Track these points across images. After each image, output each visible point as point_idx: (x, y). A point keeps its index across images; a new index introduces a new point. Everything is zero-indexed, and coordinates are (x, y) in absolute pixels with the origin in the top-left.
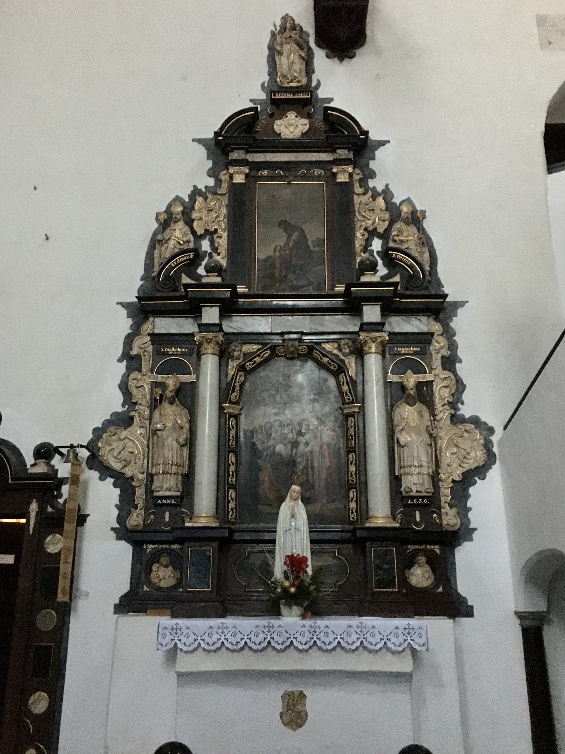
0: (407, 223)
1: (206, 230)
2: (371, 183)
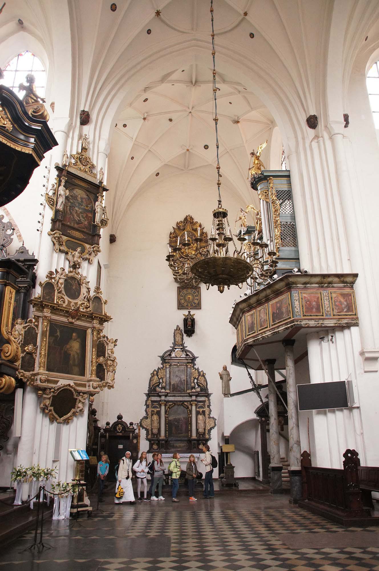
0: (202, 376)
1: (161, 377)
2: (195, 367)
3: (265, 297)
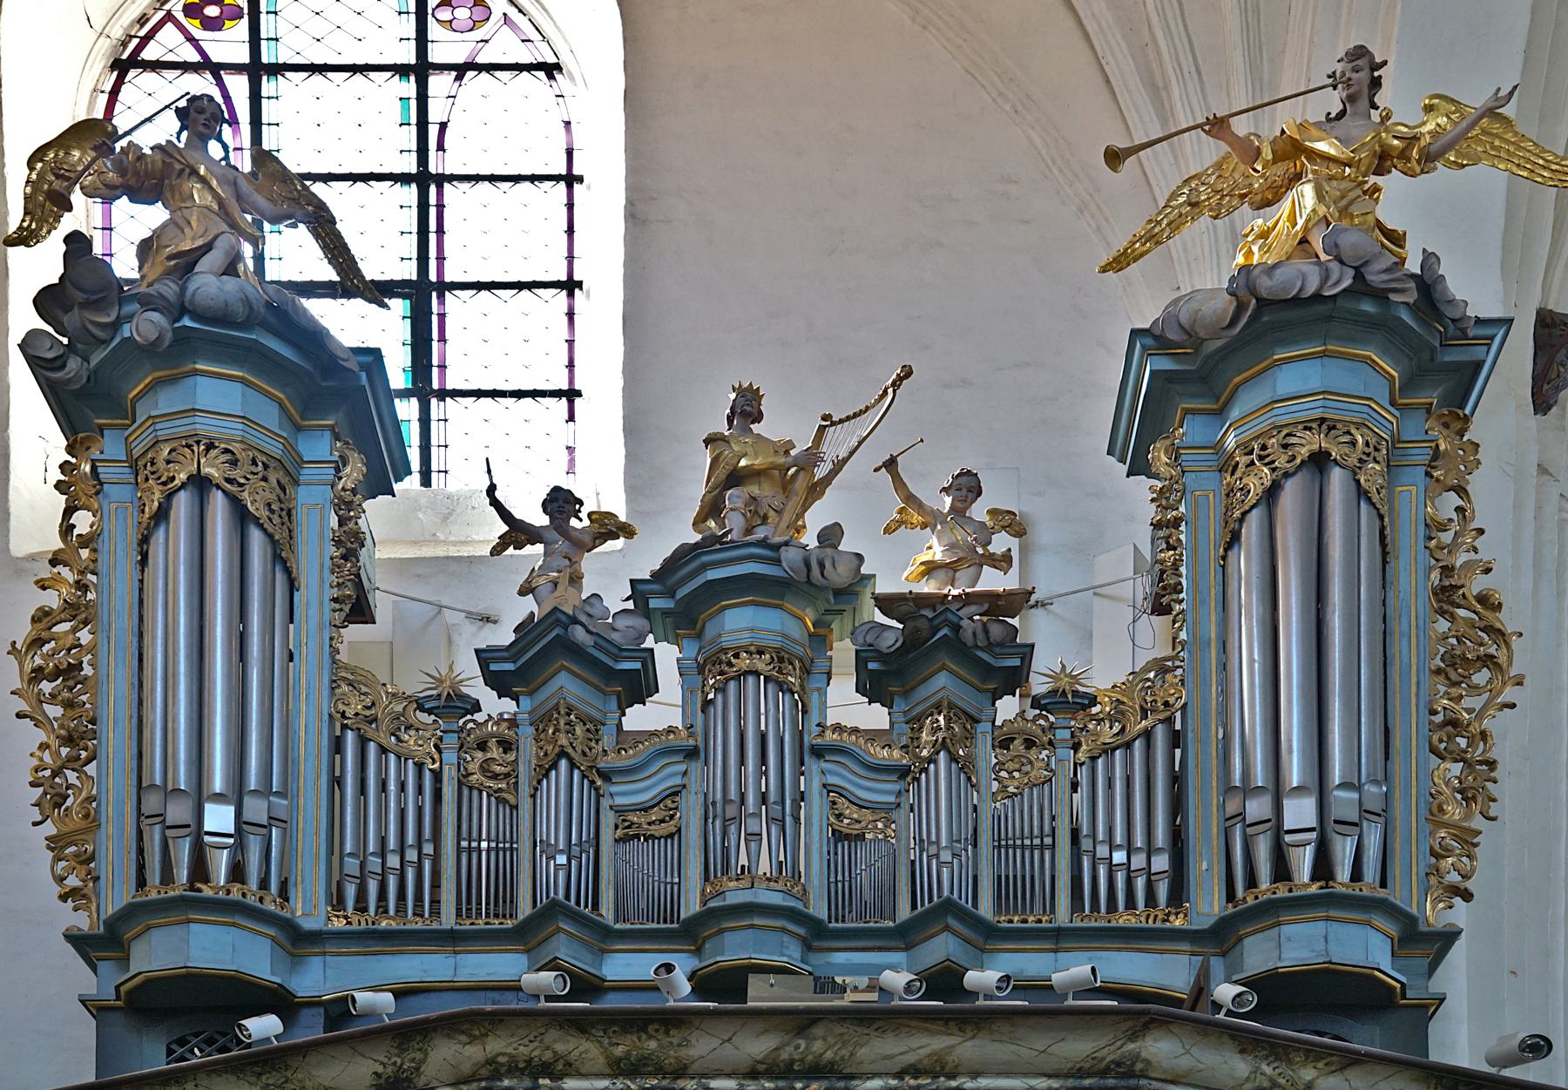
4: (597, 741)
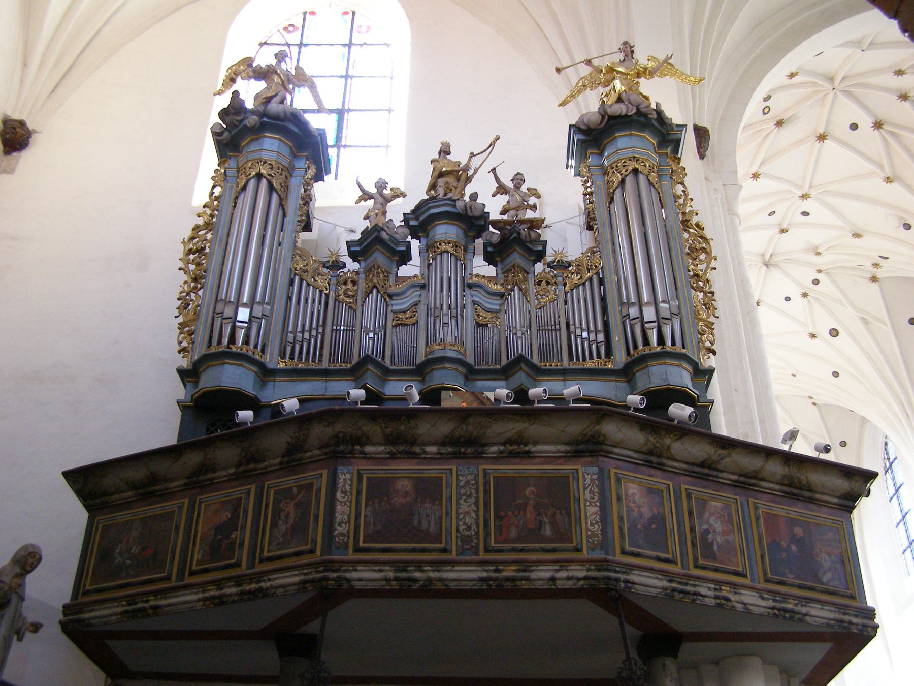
3: (741, 475)
4: (388, 281)
